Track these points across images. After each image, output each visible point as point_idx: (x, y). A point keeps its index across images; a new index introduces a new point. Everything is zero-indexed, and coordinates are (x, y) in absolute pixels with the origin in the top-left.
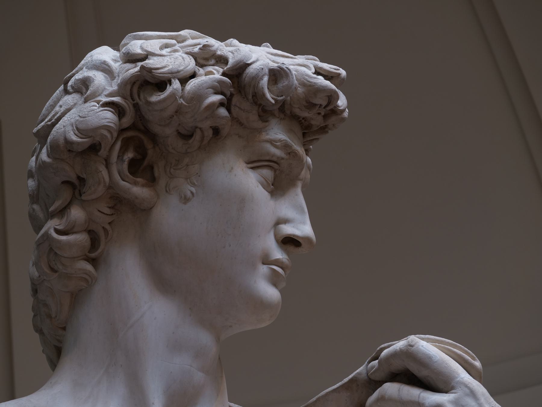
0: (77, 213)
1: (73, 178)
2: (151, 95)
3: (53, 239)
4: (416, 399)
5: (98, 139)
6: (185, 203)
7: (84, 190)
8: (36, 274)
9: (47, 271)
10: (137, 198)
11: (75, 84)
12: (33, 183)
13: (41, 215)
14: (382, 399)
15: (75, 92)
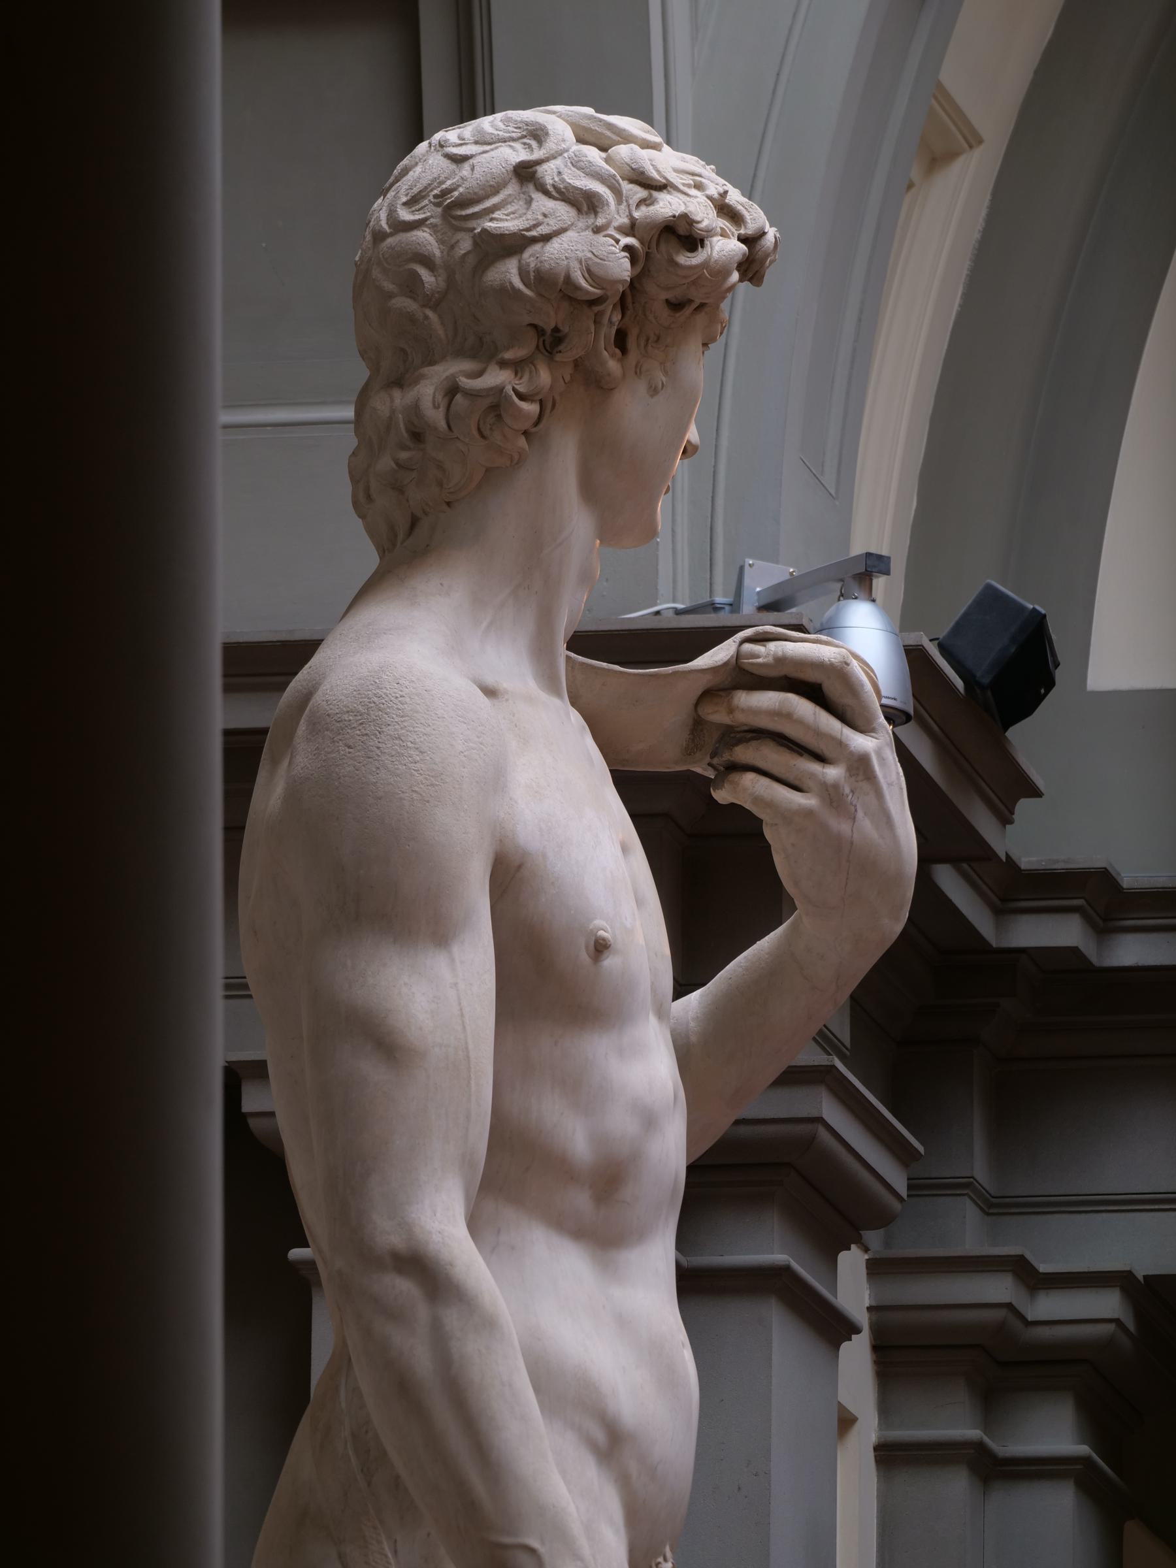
0: (544, 377)
1: (549, 325)
2: (678, 253)
3: (513, 403)
4: (839, 736)
5: (609, 293)
6: (652, 396)
7: (561, 348)
8: (442, 424)
9: (475, 433)
10: (609, 375)
11: (566, 188)
12: (433, 279)
13: (441, 332)
14: (788, 716)
15: (563, 200)
